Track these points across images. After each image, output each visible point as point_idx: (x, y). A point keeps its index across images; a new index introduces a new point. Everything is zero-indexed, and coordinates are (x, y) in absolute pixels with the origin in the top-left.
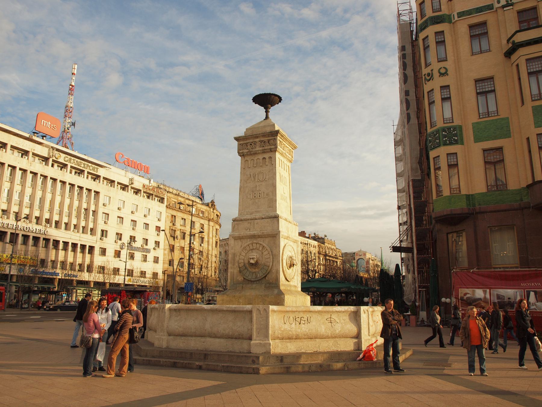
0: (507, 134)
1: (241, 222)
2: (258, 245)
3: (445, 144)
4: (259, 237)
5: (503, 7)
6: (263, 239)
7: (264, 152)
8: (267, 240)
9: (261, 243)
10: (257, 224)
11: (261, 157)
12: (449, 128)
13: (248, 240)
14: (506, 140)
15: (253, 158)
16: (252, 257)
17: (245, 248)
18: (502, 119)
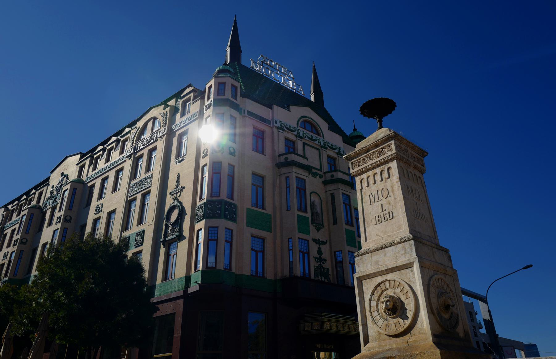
0: (268, 229)
3: (226, 217)
5: (278, 128)
12: (231, 204)
14: (268, 233)
18: (267, 215)
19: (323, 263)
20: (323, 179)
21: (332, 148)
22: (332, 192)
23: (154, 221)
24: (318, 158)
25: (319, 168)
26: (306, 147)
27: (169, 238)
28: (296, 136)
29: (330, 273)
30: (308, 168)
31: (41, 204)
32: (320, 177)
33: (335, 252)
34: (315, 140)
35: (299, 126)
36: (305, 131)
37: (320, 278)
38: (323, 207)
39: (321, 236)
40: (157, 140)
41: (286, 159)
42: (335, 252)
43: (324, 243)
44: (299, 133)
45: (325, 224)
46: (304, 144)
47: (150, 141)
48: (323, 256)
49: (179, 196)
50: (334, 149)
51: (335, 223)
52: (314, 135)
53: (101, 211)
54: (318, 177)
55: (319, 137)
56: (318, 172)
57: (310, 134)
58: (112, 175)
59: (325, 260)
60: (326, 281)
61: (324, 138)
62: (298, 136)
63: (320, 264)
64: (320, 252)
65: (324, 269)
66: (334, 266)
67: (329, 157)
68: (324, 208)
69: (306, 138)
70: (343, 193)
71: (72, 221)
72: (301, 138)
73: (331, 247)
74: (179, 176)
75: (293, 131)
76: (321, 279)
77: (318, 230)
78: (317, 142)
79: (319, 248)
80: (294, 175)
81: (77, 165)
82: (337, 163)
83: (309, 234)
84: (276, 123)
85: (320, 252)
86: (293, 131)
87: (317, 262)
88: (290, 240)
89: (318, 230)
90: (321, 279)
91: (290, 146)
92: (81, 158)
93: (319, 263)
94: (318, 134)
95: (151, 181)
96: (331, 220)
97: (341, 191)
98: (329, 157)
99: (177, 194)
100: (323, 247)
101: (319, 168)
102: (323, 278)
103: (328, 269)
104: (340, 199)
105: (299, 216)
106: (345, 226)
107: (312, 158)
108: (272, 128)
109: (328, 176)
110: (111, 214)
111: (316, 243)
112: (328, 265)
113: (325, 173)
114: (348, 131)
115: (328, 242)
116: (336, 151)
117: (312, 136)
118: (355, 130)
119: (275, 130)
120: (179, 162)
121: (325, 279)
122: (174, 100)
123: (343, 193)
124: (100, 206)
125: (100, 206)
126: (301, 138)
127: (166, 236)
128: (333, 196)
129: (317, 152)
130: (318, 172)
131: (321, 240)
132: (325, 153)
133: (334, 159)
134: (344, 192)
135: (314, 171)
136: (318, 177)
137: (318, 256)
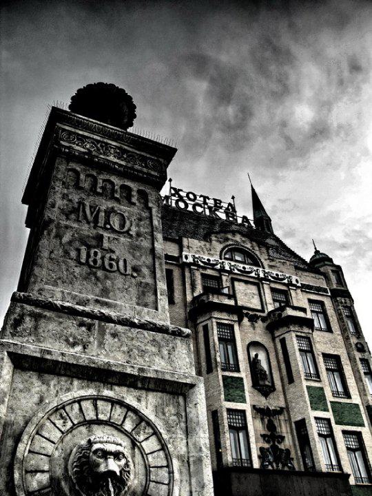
9: (134, 404)
10: (114, 335)
13: (76, 383)
16: (112, 448)
25: (259, 308)
26: (236, 283)
29: (293, 455)
34: (251, 272)
36: (233, 263)
37: (275, 465)
44: (224, 267)
46: (233, 280)
51: (291, 380)
54: (260, 322)
55: (255, 268)
56: (259, 314)
57: (241, 266)
60: (286, 469)
68: (274, 363)
70: (297, 336)
72: (227, 271)
76: (277, 466)
78: (253, 275)
83: (244, 401)
84: (186, 257)
87: (268, 442)
90: (277, 466)
96: (286, 380)
101: (259, 308)
102: (280, 465)
103: (288, 451)
104: (294, 344)
106: (305, 384)
114: (307, 256)
118: (317, 252)
121: (283, 467)
130: (259, 314)
134: (299, 334)
136: (260, 322)
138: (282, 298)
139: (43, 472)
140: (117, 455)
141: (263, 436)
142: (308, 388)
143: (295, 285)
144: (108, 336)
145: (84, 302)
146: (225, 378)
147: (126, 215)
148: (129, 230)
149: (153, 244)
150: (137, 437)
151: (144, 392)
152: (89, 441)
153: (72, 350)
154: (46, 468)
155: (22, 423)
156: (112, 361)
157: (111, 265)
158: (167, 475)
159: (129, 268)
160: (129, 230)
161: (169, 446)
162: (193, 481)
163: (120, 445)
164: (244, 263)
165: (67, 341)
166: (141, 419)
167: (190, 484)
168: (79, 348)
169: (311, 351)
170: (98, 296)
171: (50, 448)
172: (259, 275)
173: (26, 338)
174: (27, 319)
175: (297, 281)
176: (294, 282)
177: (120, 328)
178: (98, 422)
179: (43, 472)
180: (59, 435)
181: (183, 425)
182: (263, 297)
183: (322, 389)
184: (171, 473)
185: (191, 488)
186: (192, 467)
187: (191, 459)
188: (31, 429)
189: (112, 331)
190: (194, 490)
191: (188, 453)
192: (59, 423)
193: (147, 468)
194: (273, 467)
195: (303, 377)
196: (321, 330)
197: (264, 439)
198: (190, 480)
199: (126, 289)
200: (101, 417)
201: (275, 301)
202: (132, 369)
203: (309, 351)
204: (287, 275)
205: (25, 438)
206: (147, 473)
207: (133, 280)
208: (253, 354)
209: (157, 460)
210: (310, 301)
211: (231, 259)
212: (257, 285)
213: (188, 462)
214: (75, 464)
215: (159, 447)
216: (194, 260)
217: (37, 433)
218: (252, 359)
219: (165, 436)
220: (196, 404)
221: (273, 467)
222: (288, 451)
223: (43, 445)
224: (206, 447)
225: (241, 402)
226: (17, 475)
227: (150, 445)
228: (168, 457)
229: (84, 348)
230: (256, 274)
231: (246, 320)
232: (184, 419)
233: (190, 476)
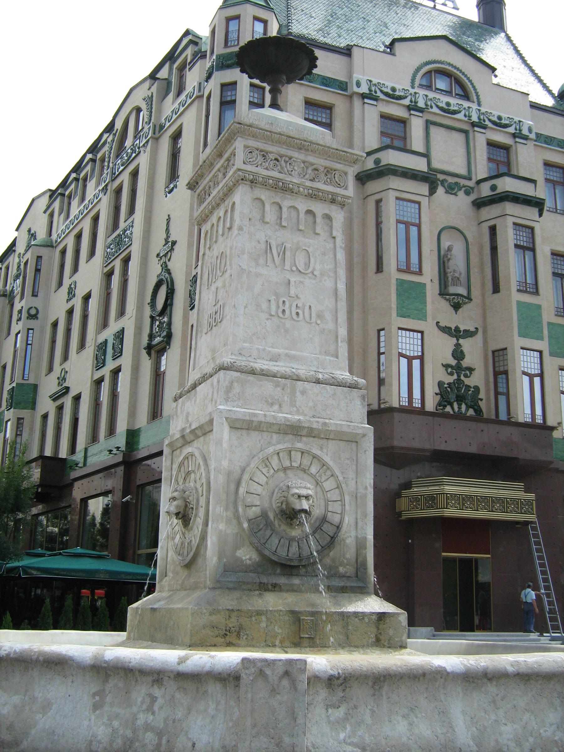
1: (251, 378)
2: (306, 461)
4: (312, 433)
5: (363, 96)
6: (321, 442)
7: (314, 195)
8: (332, 445)
10: (303, 393)
11: (302, 205)
13: (275, 436)
15: (278, 200)
16: (304, 492)
17: (266, 461)
19: (466, 376)
20: (473, 197)
21: (499, 124)
22: (491, 223)
23: (135, 311)
24: (462, 151)
25: (463, 171)
27: (157, 340)
28: (409, 108)
29: (482, 395)
30: (430, 179)
31: (8, 288)
32: (467, 193)
33: (493, 352)
34: (455, 112)
35: (417, 83)
36: (431, 95)
37: (456, 405)
38: (472, 258)
39: (464, 320)
40: (140, 152)
41: (377, 162)
42: (493, 352)
43: (468, 334)
44: (416, 102)
45: (476, 293)
46: (428, 124)
47: (130, 157)
48: (465, 363)
49: (169, 260)
50: (506, 126)
51: (496, 289)
52: (454, 102)
53: (74, 295)
54: (461, 194)
55: (466, 104)
56: (462, 182)
57: (444, 99)
58: (86, 226)
59: (471, 370)
61: (479, 105)
62: (413, 108)
63: (459, 379)
64: (458, 354)
65: (468, 387)
66: (491, 379)
67: (491, 144)
68: (474, 260)
69: (435, 110)
70: (515, 224)
71: (39, 316)
72: (421, 110)
73: (485, 342)
74: (169, 220)
75: (400, 98)
76: (460, 408)
77: (456, 307)
78: (460, 116)
79: (458, 345)
80: (392, 195)
81: (45, 212)
82: (513, 157)
84: (358, 84)
85: (458, 354)
86: (400, 98)
87: (451, 374)
88: (382, 333)
89: (456, 307)
90: (460, 408)
91: (395, 132)
92: (51, 197)
93: (455, 377)
94: (466, 96)
95: (131, 234)
97: (510, 221)
98: (491, 144)
99: (165, 255)
100: (466, 344)
102: (464, 407)
103: (477, 389)
104: (508, 238)
105: (401, 283)
106: (517, 297)
107: (448, 153)
108: (351, 97)
109: (485, 191)
110: (87, 298)
111: (451, 335)
112: (476, 380)
113: (479, 182)
115: (480, 330)
116: (511, 130)
117: (448, 104)
119: (357, 102)
120: (170, 192)
121: (467, 410)
122: (167, 66)
123: (515, 224)
124: (73, 286)
125: (73, 286)
126: (421, 110)
127: (151, 336)
128: (493, 230)
129: (460, 137)
130: (462, 182)
131: (462, 328)
132: (480, 140)
133: (506, 148)
135: (451, 180)
136: (461, 194)
137: (453, 362)
138: (501, 155)
139: (256, 506)
140: (307, 497)
141: (446, 366)
142: (519, 303)
143: (526, 138)
144: (298, 394)
145: (275, 358)
146: (401, 283)
147: (310, 250)
148: (314, 269)
149: (336, 283)
150: (319, 479)
151: (325, 440)
152: (288, 487)
153: (271, 410)
154: (258, 503)
155: (239, 471)
156: (301, 418)
157: (297, 314)
158: (340, 507)
159: (314, 315)
160: (314, 269)
161: (343, 485)
162: (359, 511)
163: (309, 489)
164: (449, 93)
165: (267, 401)
166: (324, 465)
167: (357, 513)
168: (276, 407)
169: (533, 250)
170: (287, 349)
171: (259, 490)
172: (470, 117)
173: (237, 403)
174: (235, 384)
175: (530, 130)
176: (525, 132)
177: (307, 385)
178: (291, 468)
179: (256, 506)
180: (265, 479)
181: (354, 467)
182: (472, 155)
183: (539, 307)
184: (343, 505)
185: (357, 516)
186: (359, 500)
187: (359, 495)
188: (246, 477)
189: (301, 389)
190: (359, 517)
191: (357, 489)
192: (265, 470)
193: (327, 502)
194: (453, 408)
195: (514, 287)
196: (556, 212)
197: (446, 370)
198: (357, 510)
199: (311, 339)
200: (295, 464)
201: (490, 160)
202: (317, 424)
203: (528, 248)
204: (517, 119)
205: (243, 484)
206: (326, 506)
207: (317, 327)
208: (445, 244)
209: (334, 495)
210: (547, 164)
211: (429, 87)
212: (466, 132)
213: (356, 497)
214: (278, 501)
215: (336, 486)
216: (370, 90)
217: (251, 479)
218: (442, 253)
219: (341, 478)
220: (365, 451)
221: (453, 408)
222: (477, 389)
223: (255, 488)
224: (370, 486)
225: (419, 319)
226: (240, 510)
227: (329, 485)
228: (342, 494)
229: (280, 406)
230: (465, 116)
231: (440, 190)
232: (355, 463)
233: (357, 507)
